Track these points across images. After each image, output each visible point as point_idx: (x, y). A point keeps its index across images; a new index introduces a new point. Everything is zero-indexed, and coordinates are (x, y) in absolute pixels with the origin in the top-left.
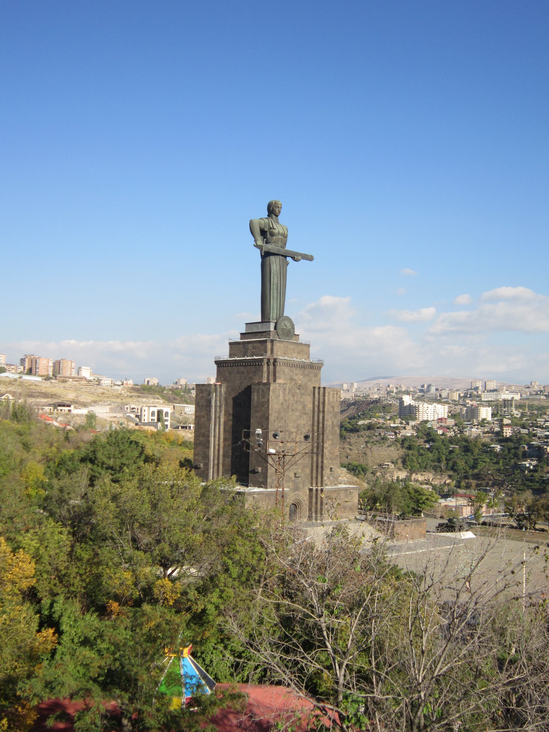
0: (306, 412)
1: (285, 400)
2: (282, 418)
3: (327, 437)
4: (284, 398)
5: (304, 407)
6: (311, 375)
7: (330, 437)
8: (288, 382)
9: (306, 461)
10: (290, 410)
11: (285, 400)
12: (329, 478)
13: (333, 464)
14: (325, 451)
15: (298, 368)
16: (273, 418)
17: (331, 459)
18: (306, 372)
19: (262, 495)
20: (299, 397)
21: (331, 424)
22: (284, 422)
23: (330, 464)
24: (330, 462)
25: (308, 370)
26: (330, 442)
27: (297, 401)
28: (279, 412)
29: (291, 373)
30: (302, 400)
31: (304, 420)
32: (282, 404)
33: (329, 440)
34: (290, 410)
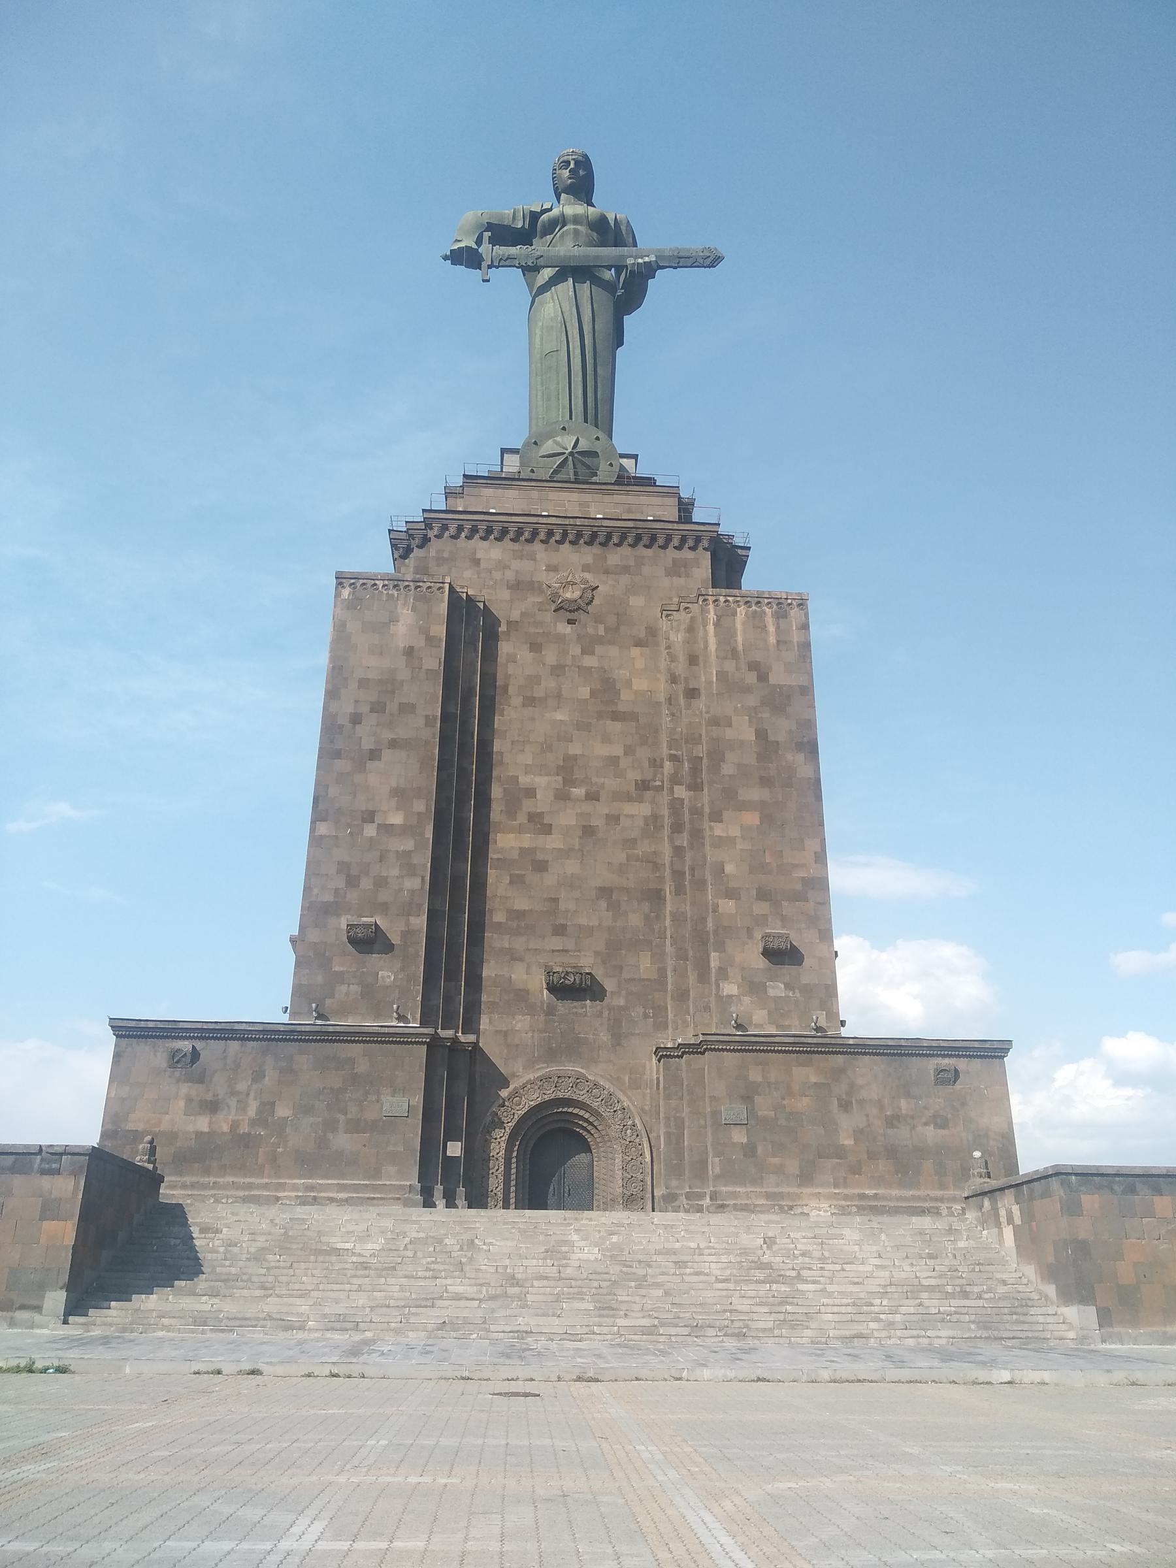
0: (622, 707)
1: (430, 640)
2: (407, 709)
3: (730, 795)
4: (425, 631)
5: (607, 689)
6: (646, 570)
7: (753, 794)
8: (506, 595)
9: (635, 920)
10: (517, 701)
11: (430, 640)
12: (755, 988)
13: (784, 920)
14: (712, 855)
15: (567, 545)
16: (349, 708)
17: (763, 895)
18: (616, 556)
19: (234, 1046)
20: (576, 650)
21: (750, 735)
22: (421, 722)
23: (762, 920)
24: (761, 908)
25: (625, 550)
26: (752, 818)
27: (558, 670)
28: (389, 684)
29: (526, 565)
30: (590, 661)
31: (606, 739)
32: (409, 652)
33: (742, 806)
34: (517, 701)
